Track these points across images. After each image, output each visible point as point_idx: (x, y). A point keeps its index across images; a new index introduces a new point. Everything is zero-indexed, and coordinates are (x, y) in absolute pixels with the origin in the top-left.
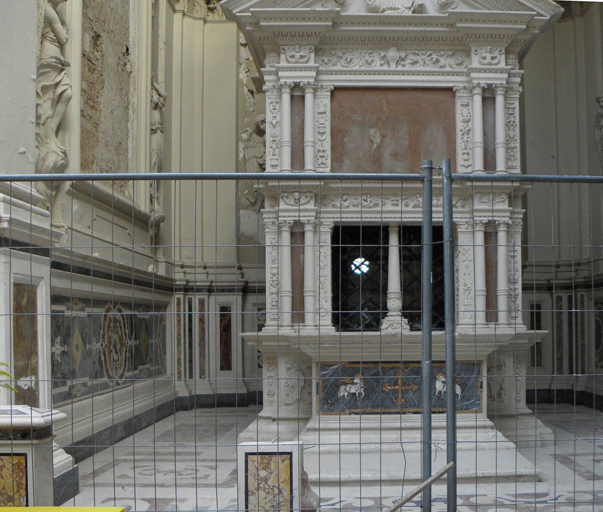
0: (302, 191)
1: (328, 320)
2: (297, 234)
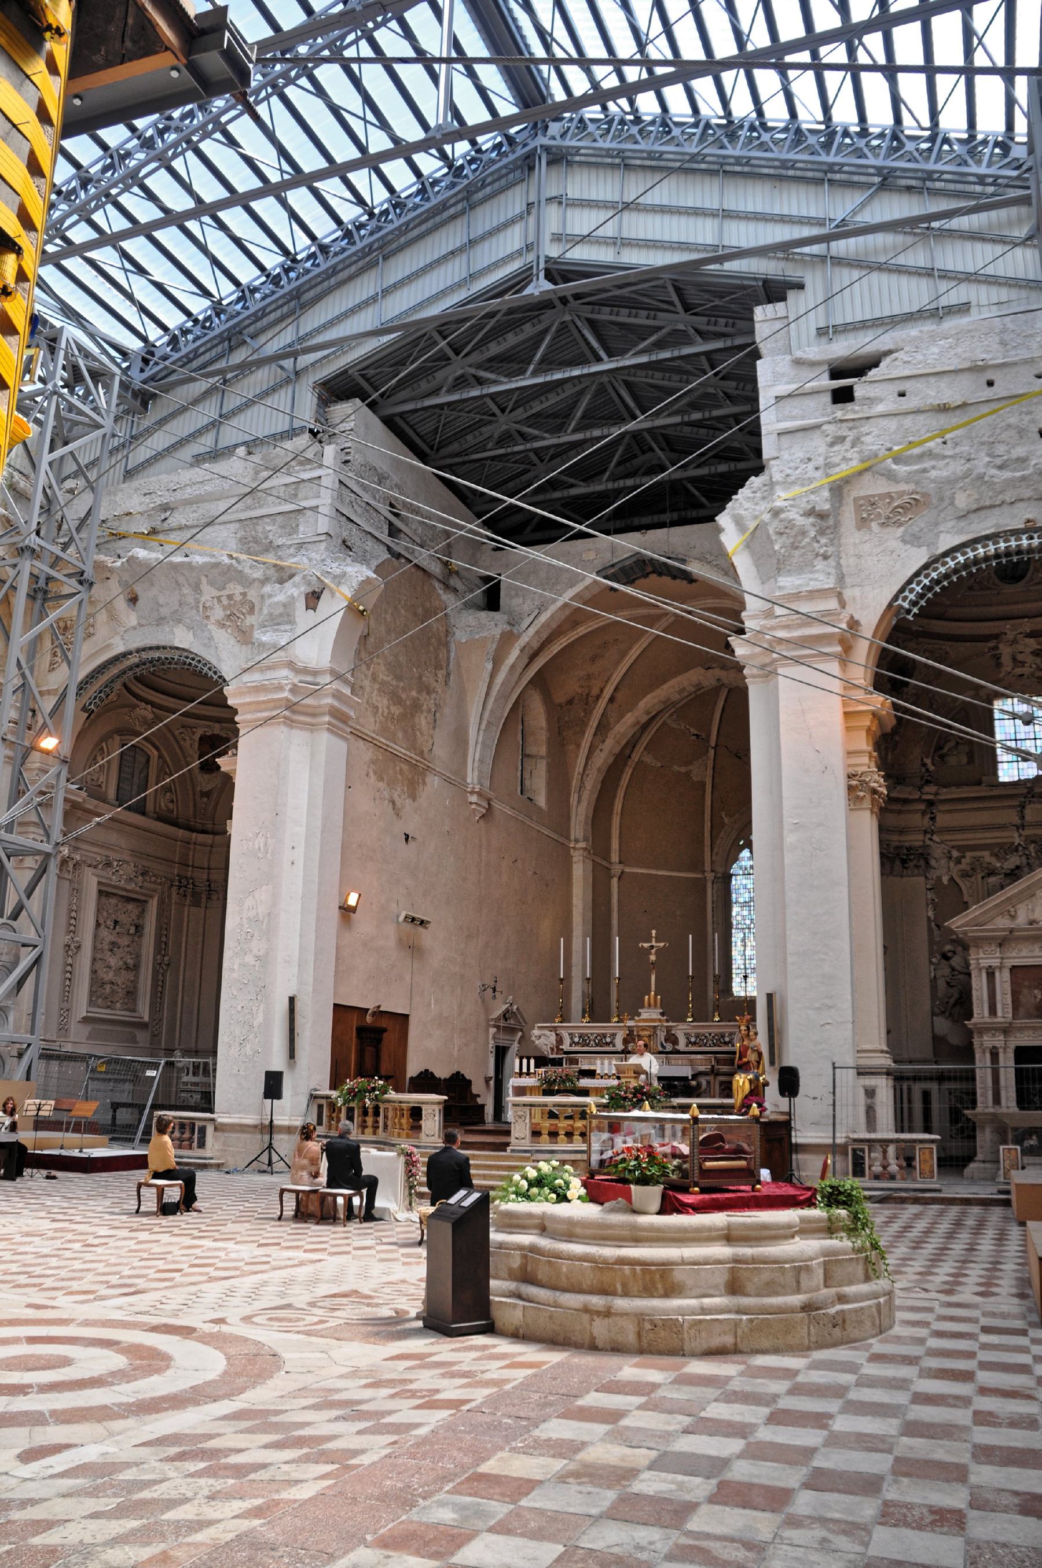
0: (996, 1029)
1: (1014, 1104)
2: (994, 1055)
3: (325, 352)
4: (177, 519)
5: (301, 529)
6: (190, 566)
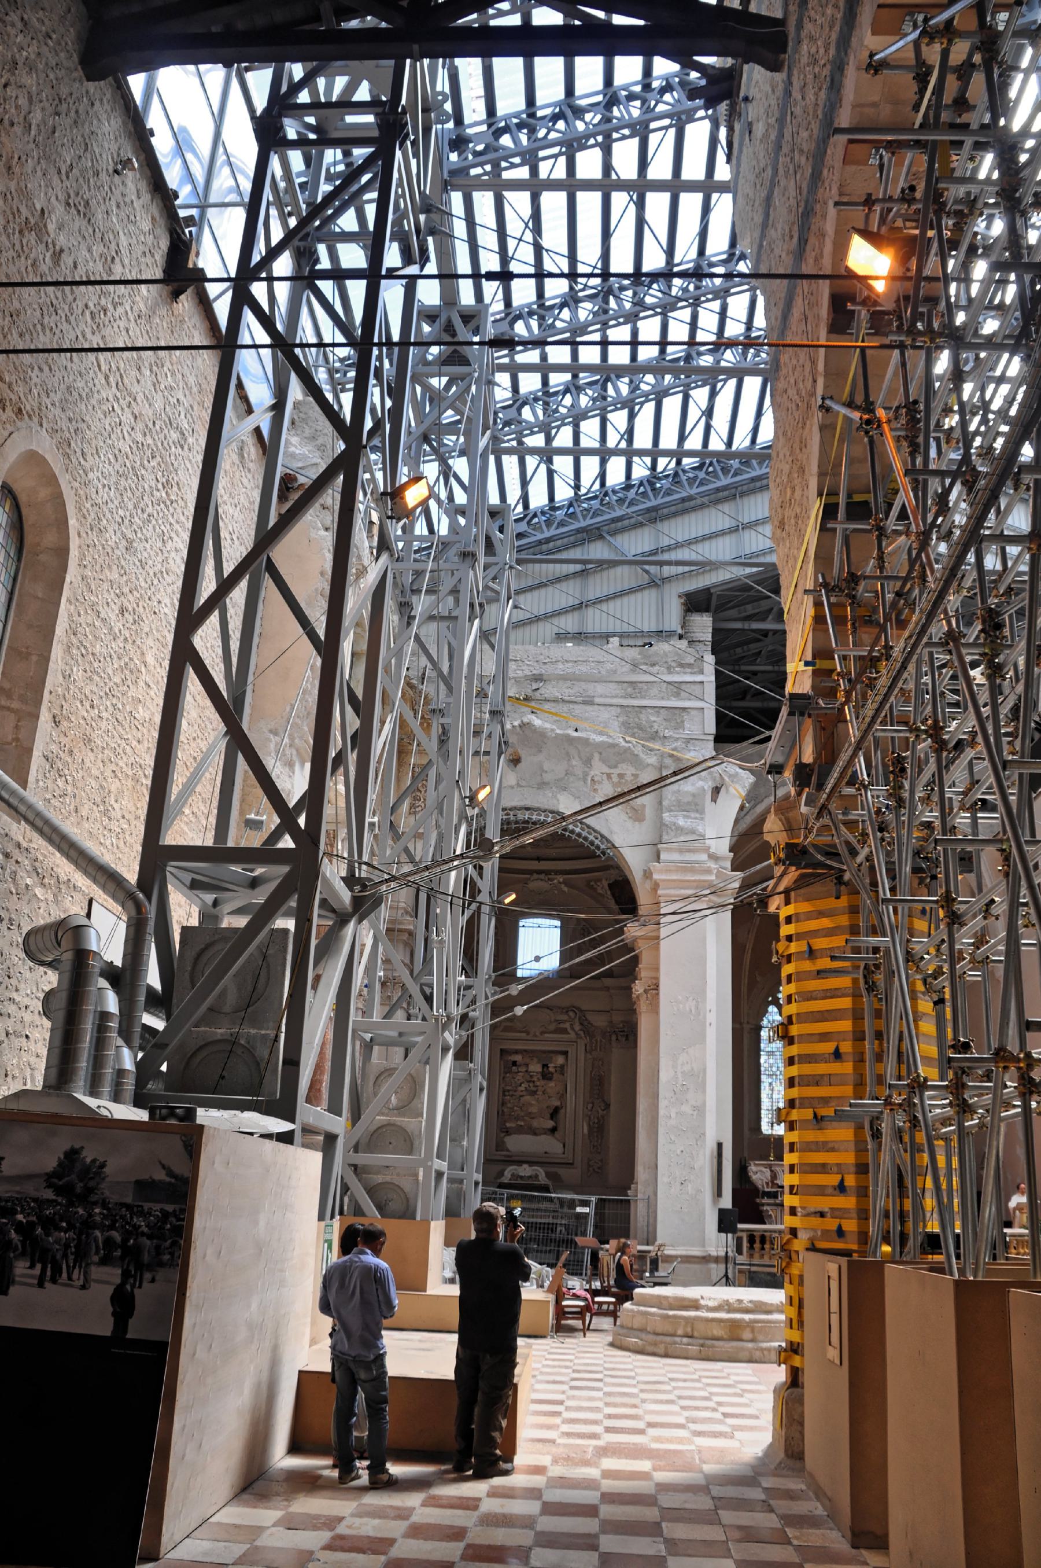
3: (687, 569)
4: (549, 690)
5: (687, 725)
6: (586, 742)
